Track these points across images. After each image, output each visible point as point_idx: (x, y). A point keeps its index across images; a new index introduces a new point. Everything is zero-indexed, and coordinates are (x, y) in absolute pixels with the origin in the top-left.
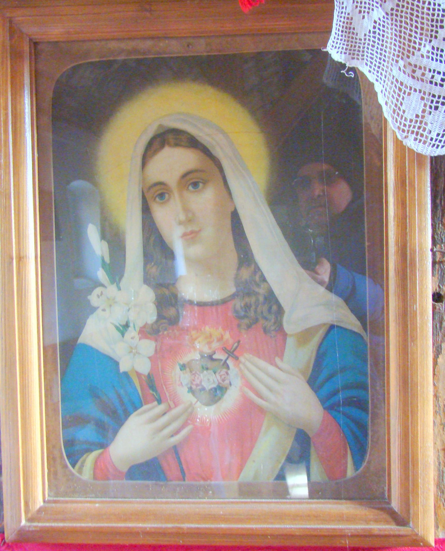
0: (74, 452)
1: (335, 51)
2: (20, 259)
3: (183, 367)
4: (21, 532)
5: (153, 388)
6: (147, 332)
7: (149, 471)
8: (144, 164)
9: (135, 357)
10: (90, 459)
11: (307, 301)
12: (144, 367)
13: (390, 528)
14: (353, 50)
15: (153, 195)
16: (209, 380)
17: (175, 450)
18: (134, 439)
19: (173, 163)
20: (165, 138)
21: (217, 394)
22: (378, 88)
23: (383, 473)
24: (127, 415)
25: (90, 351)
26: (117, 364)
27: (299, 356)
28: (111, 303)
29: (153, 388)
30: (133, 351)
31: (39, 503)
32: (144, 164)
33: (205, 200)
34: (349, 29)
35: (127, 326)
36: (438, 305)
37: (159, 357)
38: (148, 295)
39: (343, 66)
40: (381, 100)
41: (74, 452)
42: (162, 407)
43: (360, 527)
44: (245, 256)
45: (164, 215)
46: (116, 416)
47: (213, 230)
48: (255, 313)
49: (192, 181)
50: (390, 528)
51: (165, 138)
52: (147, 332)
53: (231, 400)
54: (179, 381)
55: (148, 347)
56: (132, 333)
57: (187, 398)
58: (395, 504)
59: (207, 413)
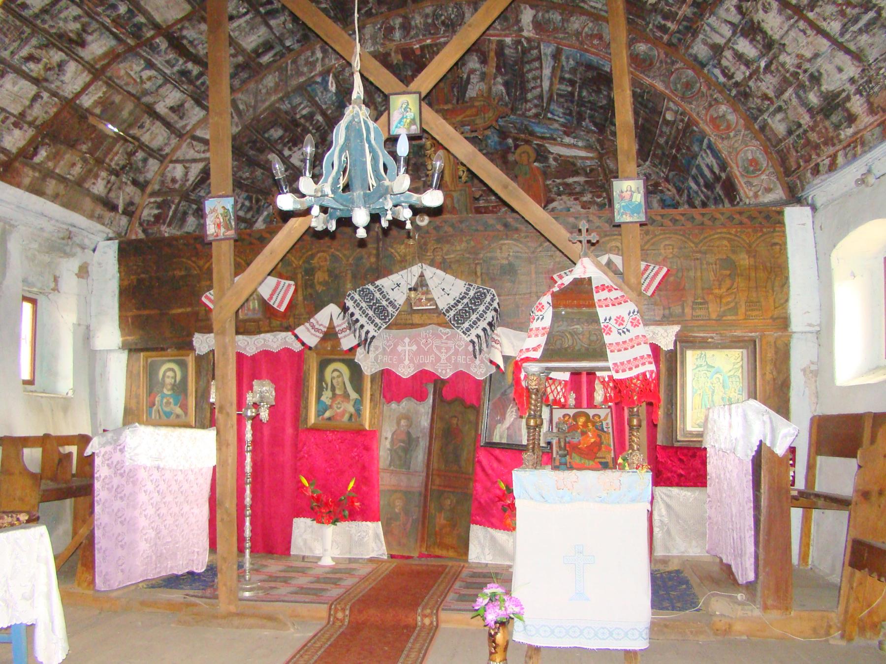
0: (319, 416)
5: (331, 407)
7: (329, 419)
9: (328, 402)
11: (354, 395)
15: (333, 378)
18: (327, 414)
19: (336, 374)
27: (352, 403)
29: (331, 407)
33: (340, 379)
41: (319, 416)
44: (345, 388)
45: (335, 382)
47: (341, 384)
48: (346, 396)
54: (335, 406)
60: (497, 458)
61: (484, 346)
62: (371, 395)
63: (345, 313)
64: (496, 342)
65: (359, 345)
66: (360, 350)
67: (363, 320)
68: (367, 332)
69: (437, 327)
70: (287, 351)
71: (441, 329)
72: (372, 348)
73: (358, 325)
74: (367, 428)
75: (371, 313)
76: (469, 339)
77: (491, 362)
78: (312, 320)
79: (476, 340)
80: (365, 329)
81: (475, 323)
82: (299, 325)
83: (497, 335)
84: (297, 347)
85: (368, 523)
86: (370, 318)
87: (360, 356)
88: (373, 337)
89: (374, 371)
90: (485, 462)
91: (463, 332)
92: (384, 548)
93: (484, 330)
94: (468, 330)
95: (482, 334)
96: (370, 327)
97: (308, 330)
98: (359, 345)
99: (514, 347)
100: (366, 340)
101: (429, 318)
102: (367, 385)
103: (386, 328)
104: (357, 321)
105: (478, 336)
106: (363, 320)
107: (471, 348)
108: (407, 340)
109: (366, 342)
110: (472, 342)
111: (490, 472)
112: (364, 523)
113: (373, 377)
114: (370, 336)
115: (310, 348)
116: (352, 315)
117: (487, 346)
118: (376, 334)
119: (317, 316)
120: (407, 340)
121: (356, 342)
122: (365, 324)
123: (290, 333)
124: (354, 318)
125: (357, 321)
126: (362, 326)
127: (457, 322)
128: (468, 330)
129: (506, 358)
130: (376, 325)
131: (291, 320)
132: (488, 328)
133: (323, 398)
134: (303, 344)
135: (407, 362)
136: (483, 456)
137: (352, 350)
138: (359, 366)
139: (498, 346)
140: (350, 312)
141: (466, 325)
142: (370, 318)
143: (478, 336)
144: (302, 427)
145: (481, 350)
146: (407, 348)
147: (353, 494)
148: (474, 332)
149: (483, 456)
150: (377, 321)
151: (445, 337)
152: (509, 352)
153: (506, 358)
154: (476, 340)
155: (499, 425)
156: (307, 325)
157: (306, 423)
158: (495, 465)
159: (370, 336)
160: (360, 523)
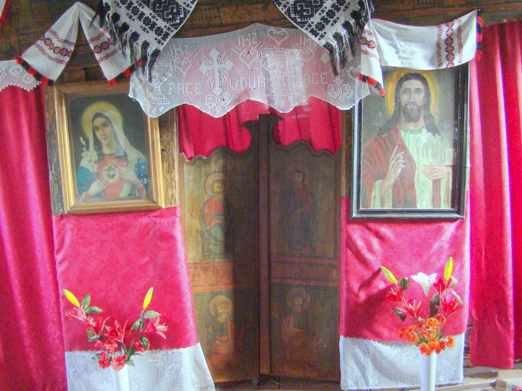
1: (131, 95)
2: (65, 146)
3: (105, 170)
4: (69, 211)
6: (96, 162)
7: (98, 195)
8: (93, 121)
9: (93, 168)
10: (84, 194)
12: (95, 171)
13: (153, 205)
14: (135, 95)
15: (95, 129)
16: (111, 173)
17: (104, 190)
18: (94, 188)
19: (99, 121)
20: (98, 115)
21: (113, 176)
22: (141, 103)
23: (152, 192)
24: (92, 183)
25: (83, 168)
26: (89, 170)
28: (87, 155)
29: (98, 176)
30: (93, 167)
31: (72, 205)
32: (93, 121)
34: (134, 91)
35: (91, 161)
36: (163, 152)
37: (99, 169)
38: (95, 153)
39: (132, 99)
40: (142, 106)
42: (100, 181)
43: (146, 205)
45: (99, 134)
46: (89, 184)
49: (104, 125)
50: (153, 205)
51: (98, 115)
52: (96, 162)
53: (116, 178)
54: (104, 173)
55: (96, 166)
56: (92, 163)
57: (106, 178)
58: (155, 200)
59: (111, 181)
60: (377, 234)
61: (349, 53)
62: (163, 150)
63: (102, 17)
64: (368, 44)
65: (132, 69)
66: (134, 78)
67: (135, 26)
68: (146, 45)
69: (263, 26)
70: (13, 90)
71: (272, 29)
72: (154, 73)
73: (129, 33)
74: (164, 207)
75: (147, 11)
76: (323, 42)
77: (364, 79)
78: (48, 35)
79: (334, 43)
80: (140, 41)
81: (331, 14)
82: (28, 45)
83: (370, 34)
84: (28, 83)
85: (182, 350)
86: (147, 21)
87: (138, 90)
88: (156, 53)
89: (163, 110)
90: (360, 243)
91: (313, 32)
92: (210, 377)
93: (346, 25)
94: (320, 27)
95: (343, 32)
96: (150, 37)
97: (44, 53)
98: (132, 69)
99: (397, 53)
100: (144, 58)
101: (250, 13)
102: (155, 135)
103: (176, 36)
104: (125, 27)
105: (337, 36)
106: (135, 26)
107: (325, 57)
108: (214, 53)
109: (145, 61)
110: (327, 46)
111: (368, 256)
112: (175, 350)
113: (163, 121)
114: (150, 51)
115: (50, 83)
116: (116, 17)
117: (353, 53)
118: (161, 48)
119: (53, 28)
120: (214, 53)
121: (128, 64)
122: (140, 31)
123: (14, 61)
124: (120, 24)
125: (125, 27)
126: (135, 36)
127: (300, 13)
128: (320, 27)
129: (387, 72)
130: (159, 31)
131: (13, 39)
132: (352, 22)
133: (84, 163)
134: (38, 76)
135: (217, 91)
136: (358, 236)
137: (123, 78)
138: (137, 104)
139: (374, 51)
140: (111, 13)
141: (316, 19)
142: (147, 21)
143: (337, 36)
144: (56, 212)
145: (343, 61)
146: (216, 66)
147: (153, 314)
148: (330, 31)
149: (358, 236)
150: (161, 23)
151: (279, 43)
152: (393, 61)
153: (387, 72)
154: (334, 43)
155: (378, 183)
156: (39, 42)
157: (63, 207)
158: (375, 242)
159: (150, 51)
160: (170, 352)
